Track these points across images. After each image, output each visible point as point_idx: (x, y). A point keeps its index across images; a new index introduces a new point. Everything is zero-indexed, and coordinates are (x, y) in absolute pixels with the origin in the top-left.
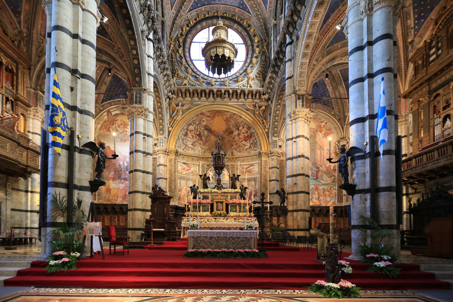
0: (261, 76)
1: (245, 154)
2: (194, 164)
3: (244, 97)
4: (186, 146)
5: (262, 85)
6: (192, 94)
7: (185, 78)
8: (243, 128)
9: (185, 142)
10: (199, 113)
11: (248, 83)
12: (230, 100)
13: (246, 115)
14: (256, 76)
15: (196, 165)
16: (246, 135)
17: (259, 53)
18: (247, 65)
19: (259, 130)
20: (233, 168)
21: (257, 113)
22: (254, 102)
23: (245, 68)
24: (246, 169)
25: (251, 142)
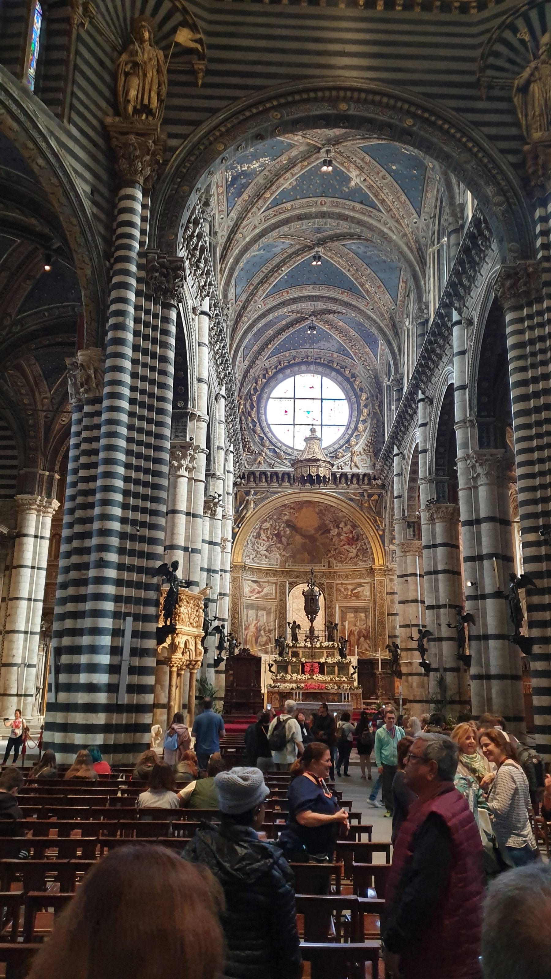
1: (348, 567)
2: (268, 582)
4: (257, 552)
5: (373, 463)
6: (269, 479)
7: (260, 454)
8: (346, 525)
9: (256, 548)
10: (279, 505)
11: (352, 461)
13: (349, 507)
14: (364, 450)
16: (351, 536)
17: (368, 415)
18: (350, 432)
20: (331, 588)
21: (366, 505)
22: (360, 488)
23: (347, 437)
24: (351, 592)
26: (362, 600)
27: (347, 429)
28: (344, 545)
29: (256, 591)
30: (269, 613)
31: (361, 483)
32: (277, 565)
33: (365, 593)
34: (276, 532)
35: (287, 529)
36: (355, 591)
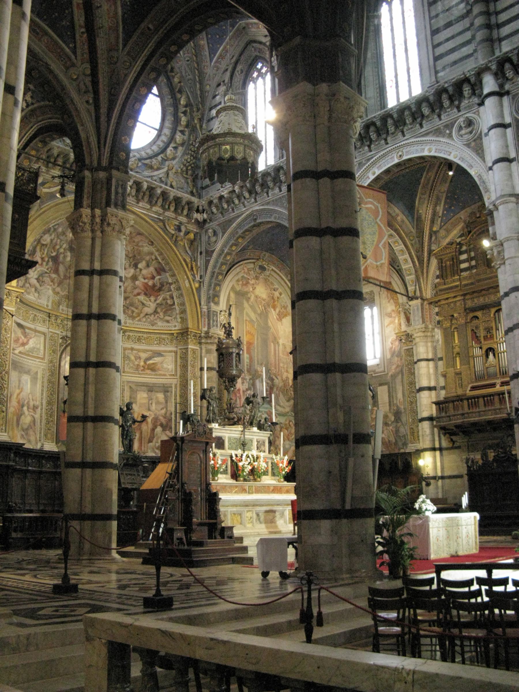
0: (190, 172)
3: (163, 207)
8: (148, 266)
12: (138, 203)
15: (39, 332)
16: (150, 283)
17: (187, 126)
19: (184, 281)
22: (176, 219)
24: (145, 362)
25: (158, 302)
26: (160, 375)
27: (159, 136)
28: (139, 294)
29: (21, 341)
30: (34, 379)
31: (180, 211)
32: (47, 306)
33: (165, 366)
34: (54, 254)
35: (69, 254)
36: (151, 362)
